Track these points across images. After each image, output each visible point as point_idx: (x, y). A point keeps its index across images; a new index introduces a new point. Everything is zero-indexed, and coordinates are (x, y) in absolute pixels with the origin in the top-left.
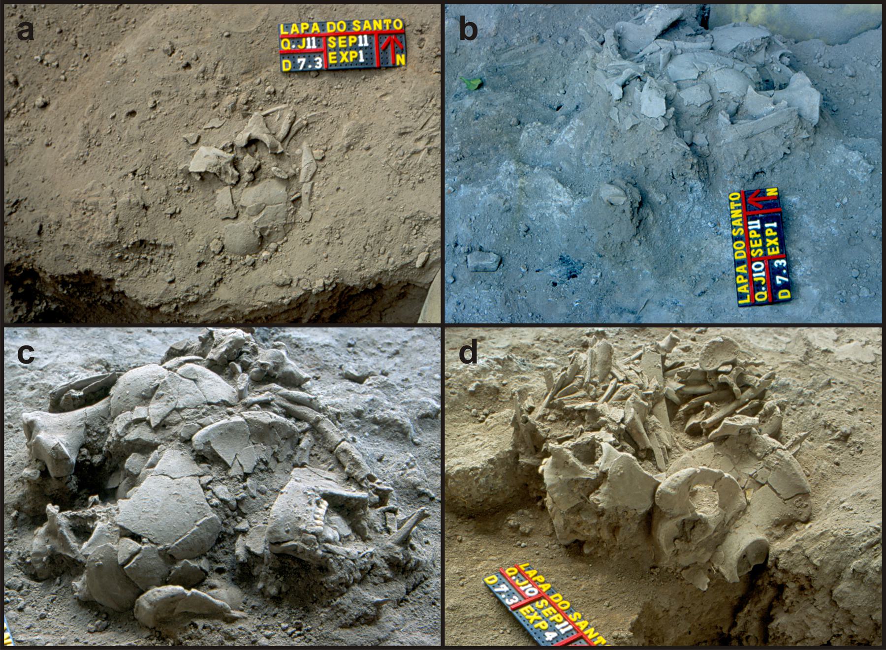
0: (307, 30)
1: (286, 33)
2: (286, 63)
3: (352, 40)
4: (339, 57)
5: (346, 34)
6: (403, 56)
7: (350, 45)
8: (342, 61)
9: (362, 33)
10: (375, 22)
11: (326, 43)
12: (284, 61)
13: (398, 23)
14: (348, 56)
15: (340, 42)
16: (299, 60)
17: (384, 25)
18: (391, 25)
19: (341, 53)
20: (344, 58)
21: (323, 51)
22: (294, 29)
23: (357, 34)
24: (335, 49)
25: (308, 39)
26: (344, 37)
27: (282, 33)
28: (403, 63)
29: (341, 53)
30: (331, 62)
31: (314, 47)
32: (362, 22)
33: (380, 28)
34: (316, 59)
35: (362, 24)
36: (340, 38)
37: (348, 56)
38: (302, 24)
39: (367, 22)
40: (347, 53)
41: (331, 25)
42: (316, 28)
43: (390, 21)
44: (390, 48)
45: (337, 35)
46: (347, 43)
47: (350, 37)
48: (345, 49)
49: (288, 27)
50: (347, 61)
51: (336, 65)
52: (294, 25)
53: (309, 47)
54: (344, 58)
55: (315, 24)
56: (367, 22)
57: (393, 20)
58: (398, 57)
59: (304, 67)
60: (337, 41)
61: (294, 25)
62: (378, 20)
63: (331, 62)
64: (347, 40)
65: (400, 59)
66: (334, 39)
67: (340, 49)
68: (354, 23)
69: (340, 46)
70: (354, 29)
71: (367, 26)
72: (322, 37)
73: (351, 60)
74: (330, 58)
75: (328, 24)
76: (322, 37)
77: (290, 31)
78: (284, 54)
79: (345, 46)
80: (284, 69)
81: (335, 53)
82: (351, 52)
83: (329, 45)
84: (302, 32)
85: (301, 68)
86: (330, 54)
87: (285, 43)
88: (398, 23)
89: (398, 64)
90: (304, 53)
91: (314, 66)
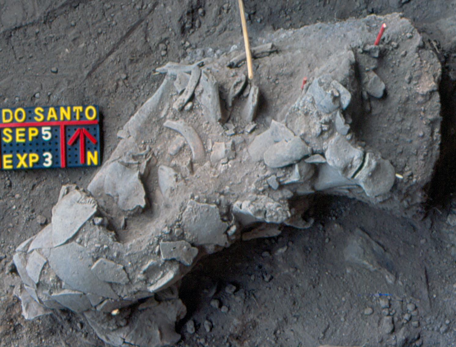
5: (26, 126)
6: (96, 153)
7: (30, 139)
10: (62, 110)
13: (90, 112)
15: (18, 135)
17: (73, 114)
18: (82, 115)
26: (23, 130)
28: (95, 162)
32: (46, 109)
33: (68, 117)
35: (45, 114)
39: (52, 109)
43: (81, 108)
44: (80, 142)
45: (14, 126)
46: (26, 137)
47: (30, 130)
56: (52, 109)
57: (84, 107)
58: (89, 154)
60: (13, 135)
62: (65, 108)
64: (26, 133)
65: (92, 157)
66: (10, 131)
68: (36, 111)
69: (18, 140)
70: (36, 118)
71: (52, 114)
75: (4, 111)
79: (23, 141)
83: (4, 139)
88: (90, 112)
89: (89, 163)
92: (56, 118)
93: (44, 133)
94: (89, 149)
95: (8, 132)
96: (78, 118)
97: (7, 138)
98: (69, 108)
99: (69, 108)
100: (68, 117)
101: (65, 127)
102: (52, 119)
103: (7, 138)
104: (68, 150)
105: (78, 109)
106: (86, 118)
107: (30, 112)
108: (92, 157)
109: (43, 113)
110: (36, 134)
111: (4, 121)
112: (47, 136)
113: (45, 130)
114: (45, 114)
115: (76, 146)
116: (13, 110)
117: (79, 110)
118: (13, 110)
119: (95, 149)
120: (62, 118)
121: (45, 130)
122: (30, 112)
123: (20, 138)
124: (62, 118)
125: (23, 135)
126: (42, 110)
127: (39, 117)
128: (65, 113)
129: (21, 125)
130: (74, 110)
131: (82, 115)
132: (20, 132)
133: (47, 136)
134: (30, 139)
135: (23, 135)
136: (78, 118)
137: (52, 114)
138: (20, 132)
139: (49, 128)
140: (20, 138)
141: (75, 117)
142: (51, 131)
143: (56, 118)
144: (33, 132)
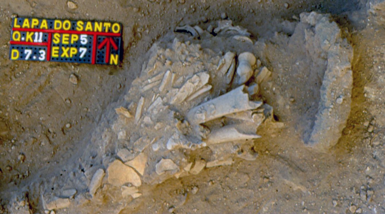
0: (37, 26)
1: (19, 26)
2: (15, 55)
3: (74, 38)
4: (61, 52)
6: (117, 56)
7: (72, 42)
8: (63, 56)
9: (83, 32)
10: (96, 24)
11: (51, 38)
12: (14, 51)
13: (116, 28)
14: (69, 52)
15: (64, 39)
16: (26, 51)
17: (104, 28)
18: (110, 30)
19: (63, 48)
20: (65, 54)
21: (48, 44)
22: (26, 24)
23: (79, 33)
24: (58, 45)
25: (36, 34)
26: (68, 35)
27: (16, 26)
29: (63, 48)
30: (54, 55)
31: (40, 41)
32: (85, 21)
33: (100, 30)
34: (41, 51)
35: (84, 26)
36: (64, 35)
37: (69, 52)
38: (34, 20)
39: (89, 24)
40: (68, 49)
41: (58, 25)
42: (44, 25)
45: (62, 32)
46: (70, 41)
47: (73, 36)
48: (67, 46)
49: (20, 22)
50: (67, 56)
51: (57, 59)
52: (26, 20)
53: (36, 41)
54: (65, 54)
55: (44, 21)
56: (89, 24)
57: (112, 23)
58: (112, 57)
59: (31, 57)
60: (61, 39)
61: (26, 20)
62: (99, 22)
63: (54, 55)
64: (70, 38)
66: (59, 35)
67: (63, 45)
69: (64, 42)
70: (78, 29)
71: (89, 27)
72: (49, 34)
73: (71, 56)
74: (53, 52)
75: (56, 22)
76: (49, 34)
77: (21, 25)
78: (14, 45)
79: (67, 43)
80: (13, 58)
81: (57, 48)
82: (72, 49)
83: (54, 41)
84: (32, 27)
85: (27, 58)
86: (54, 48)
87: (16, 36)
88: (116, 28)
89: (111, 63)
90: (30, 45)
91: (37, 58)
92: (91, 30)
93: (82, 39)
94: (113, 53)
95: (57, 36)
96: (107, 31)
97: (56, 40)
98: (101, 24)
99: (101, 24)
100: (100, 30)
101: (97, 36)
102: (89, 31)
103: (56, 40)
104: (97, 52)
105: (107, 25)
106: (112, 32)
107: (74, 24)
108: (114, 59)
109: (82, 25)
110: (76, 39)
111: (56, 28)
112: (84, 41)
113: (83, 37)
114: (84, 26)
115: (103, 50)
116: (63, 20)
117: (108, 26)
118: (63, 20)
119: (117, 53)
120: (95, 30)
121: (83, 37)
122: (74, 24)
123: (65, 41)
124: (95, 30)
125: (67, 39)
126: (82, 23)
127: (80, 28)
128: (98, 27)
129: (66, 32)
130: (105, 25)
131: (110, 30)
132: (66, 37)
133: (84, 41)
134: (72, 42)
135: (67, 39)
136: (107, 31)
137: (89, 26)
138: (66, 37)
139: (86, 36)
140: (65, 41)
141: (105, 30)
142: (87, 38)
143: (91, 30)
144: (75, 38)
